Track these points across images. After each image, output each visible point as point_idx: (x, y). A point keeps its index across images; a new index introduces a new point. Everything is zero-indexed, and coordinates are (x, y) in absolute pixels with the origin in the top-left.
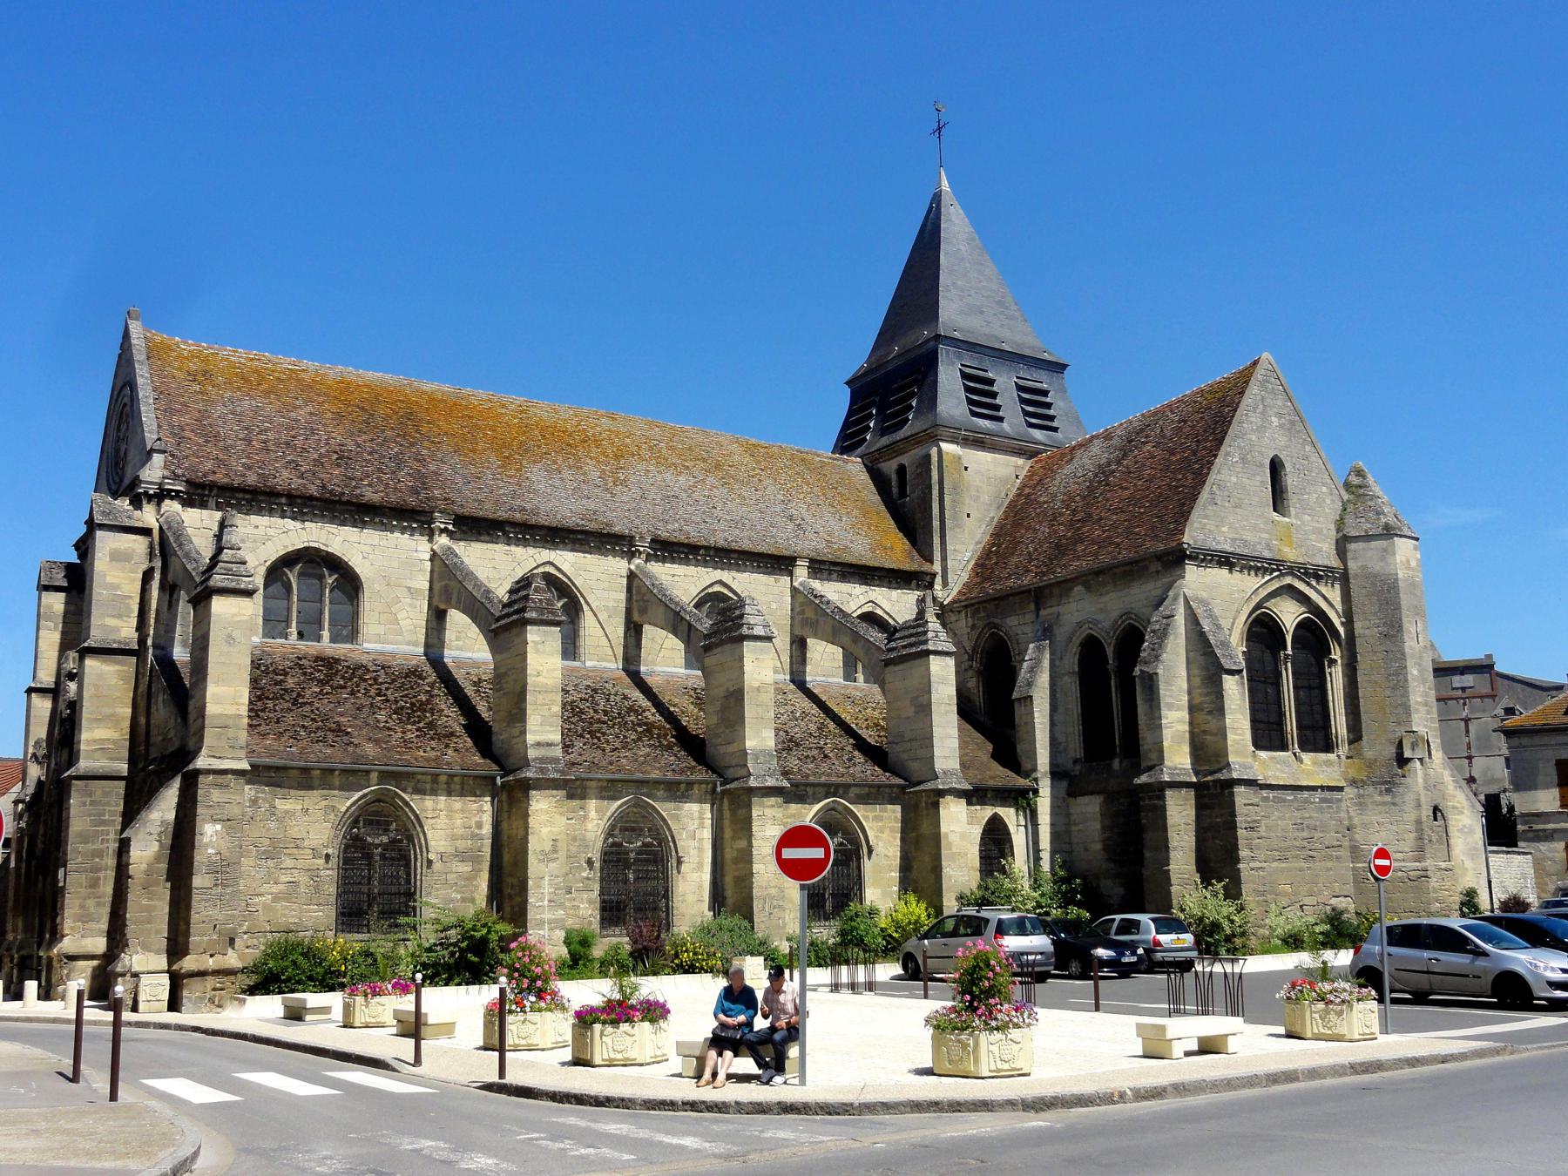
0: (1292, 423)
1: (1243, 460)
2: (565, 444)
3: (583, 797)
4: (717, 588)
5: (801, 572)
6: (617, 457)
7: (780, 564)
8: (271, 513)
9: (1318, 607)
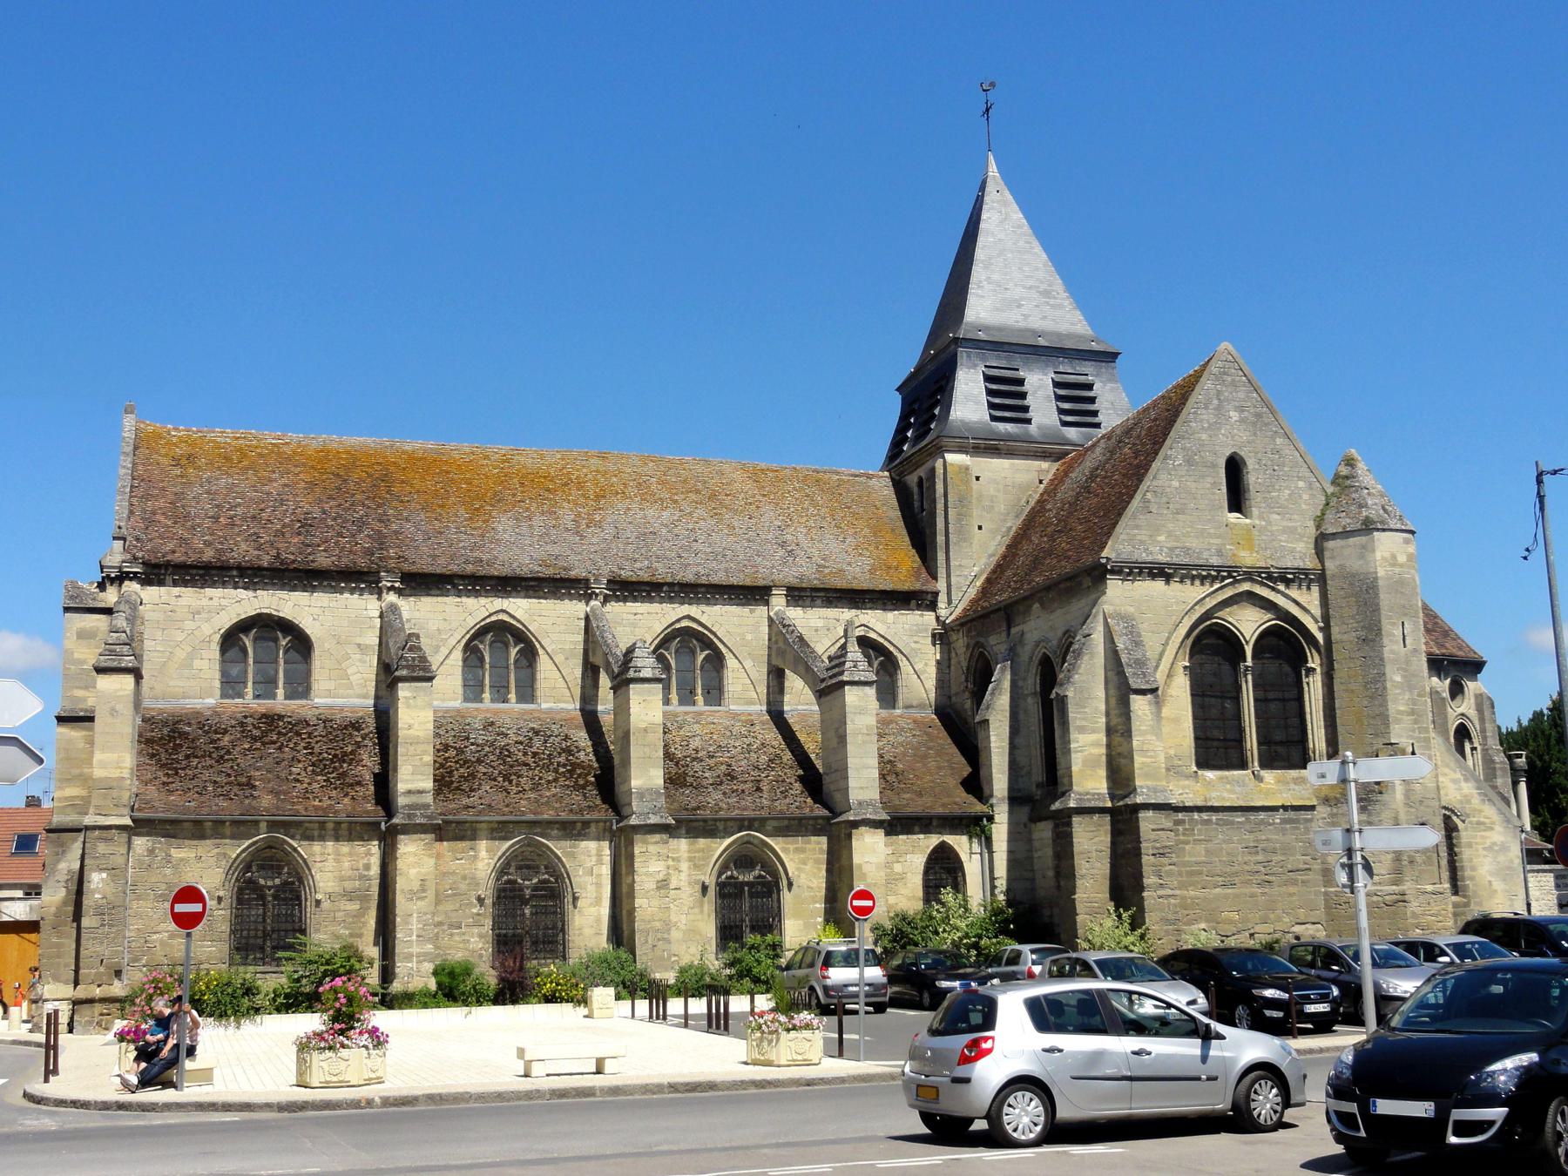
0: (1258, 415)
1: (1189, 462)
2: (542, 488)
3: (474, 838)
4: (685, 623)
5: (778, 601)
6: (598, 497)
7: (755, 594)
8: (224, 585)
9: (1288, 613)
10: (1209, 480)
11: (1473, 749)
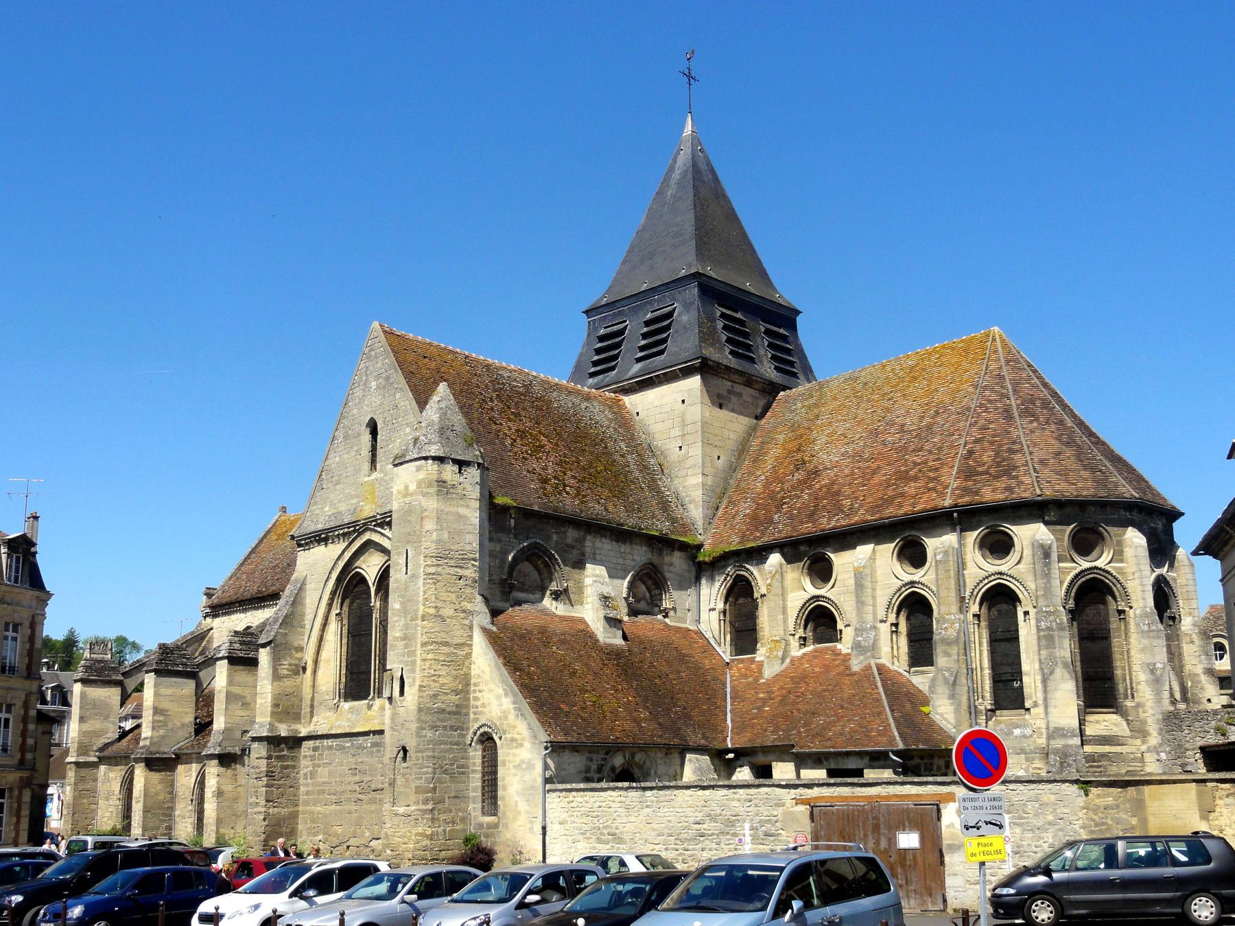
1: (346, 438)
10: (355, 448)
11: (1026, 613)
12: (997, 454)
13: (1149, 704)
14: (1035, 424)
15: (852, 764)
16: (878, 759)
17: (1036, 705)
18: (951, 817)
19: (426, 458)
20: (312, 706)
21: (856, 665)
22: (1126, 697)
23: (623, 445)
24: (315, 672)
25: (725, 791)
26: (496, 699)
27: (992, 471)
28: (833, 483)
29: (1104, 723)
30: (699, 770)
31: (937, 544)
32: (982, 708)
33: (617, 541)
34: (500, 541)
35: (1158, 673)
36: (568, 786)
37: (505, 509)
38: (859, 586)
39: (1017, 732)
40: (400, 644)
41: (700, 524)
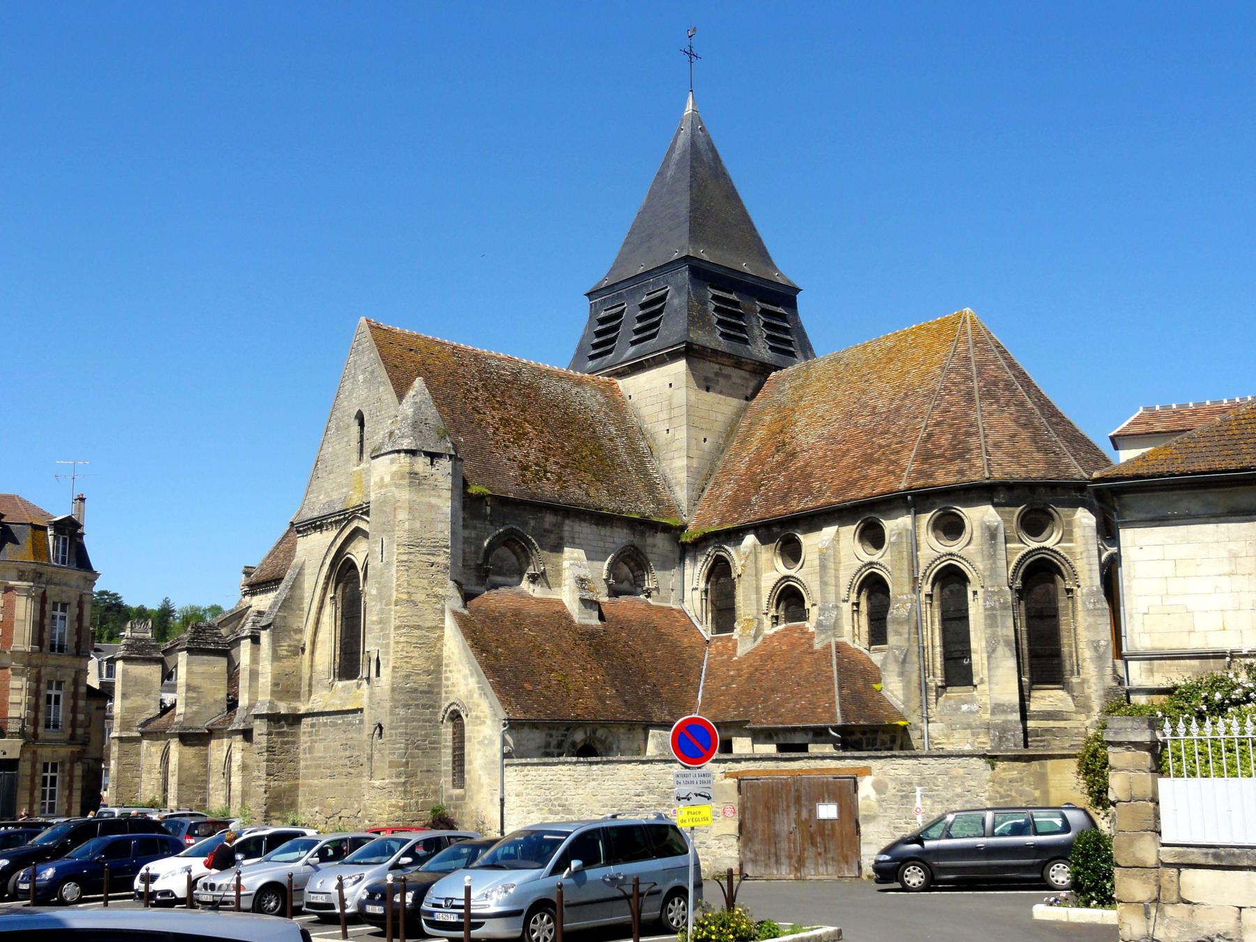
1: (337, 429)
11: (975, 593)
12: (955, 436)
13: (1093, 680)
14: (995, 406)
15: (798, 739)
16: (820, 734)
17: (982, 682)
18: (866, 788)
19: (399, 452)
20: (310, 685)
21: (818, 645)
22: (1072, 674)
23: (612, 429)
24: (312, 653)
25: (661, 766)
26: (464, 680)
27: (948, 454)
28: (807, 465)
29: (1046, 699)
30: (662, 745)
31: (895, 525)
32: (932, 684)
33: (597, 524)
34: (475, 528)
35: (1102, 650)
36: (524, 761)
37: (480, 498)
38: (823, 567)
39: (965, 708)
40: (377, 627)
41: (684, 505)
